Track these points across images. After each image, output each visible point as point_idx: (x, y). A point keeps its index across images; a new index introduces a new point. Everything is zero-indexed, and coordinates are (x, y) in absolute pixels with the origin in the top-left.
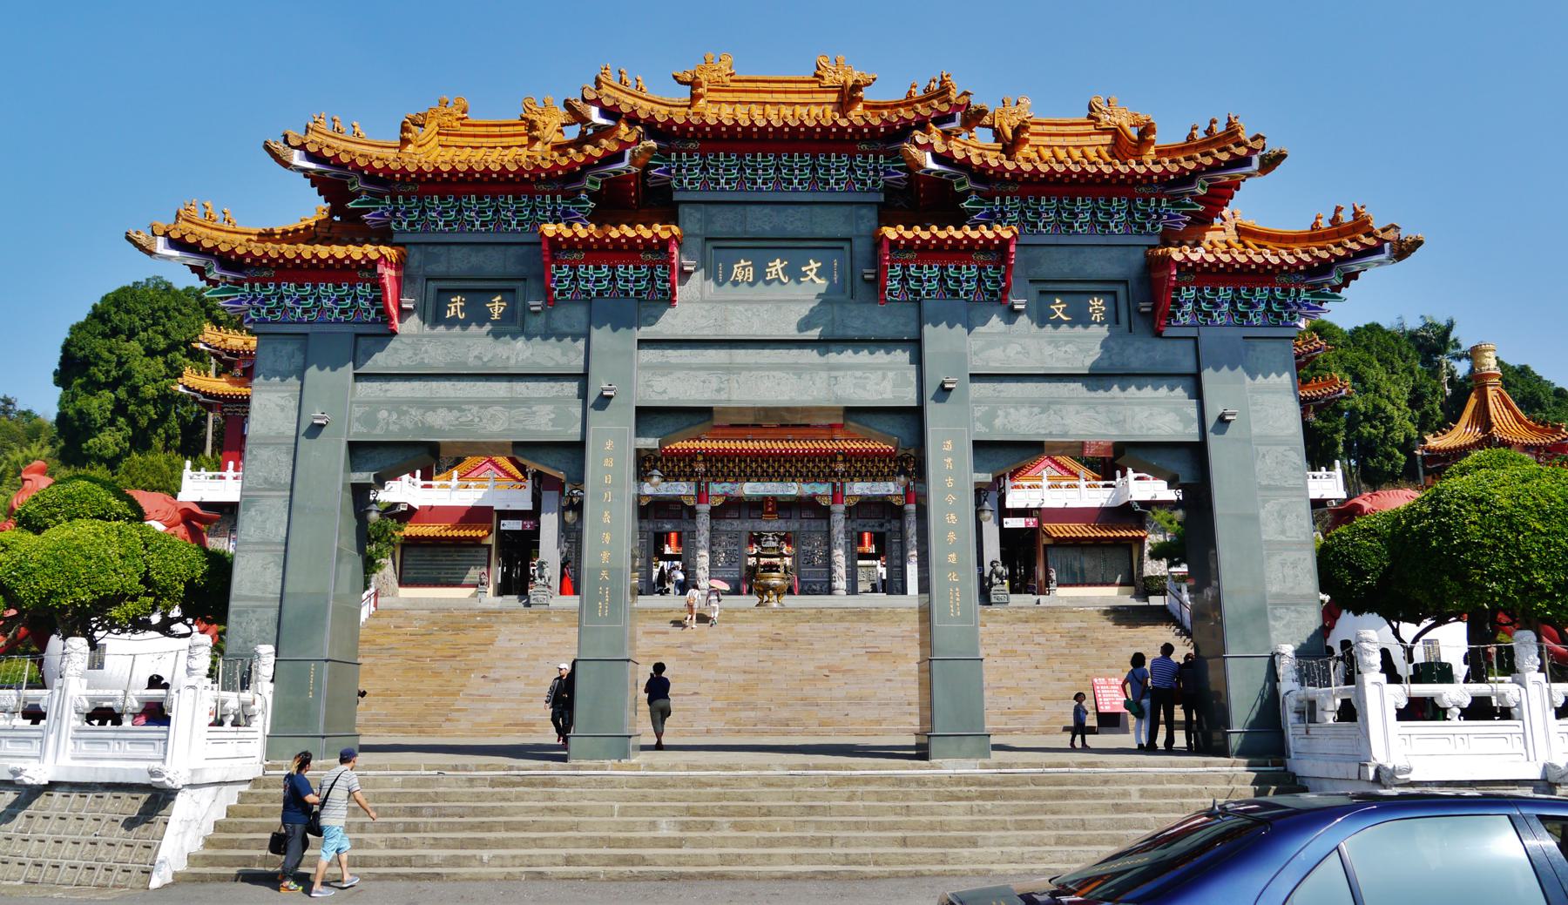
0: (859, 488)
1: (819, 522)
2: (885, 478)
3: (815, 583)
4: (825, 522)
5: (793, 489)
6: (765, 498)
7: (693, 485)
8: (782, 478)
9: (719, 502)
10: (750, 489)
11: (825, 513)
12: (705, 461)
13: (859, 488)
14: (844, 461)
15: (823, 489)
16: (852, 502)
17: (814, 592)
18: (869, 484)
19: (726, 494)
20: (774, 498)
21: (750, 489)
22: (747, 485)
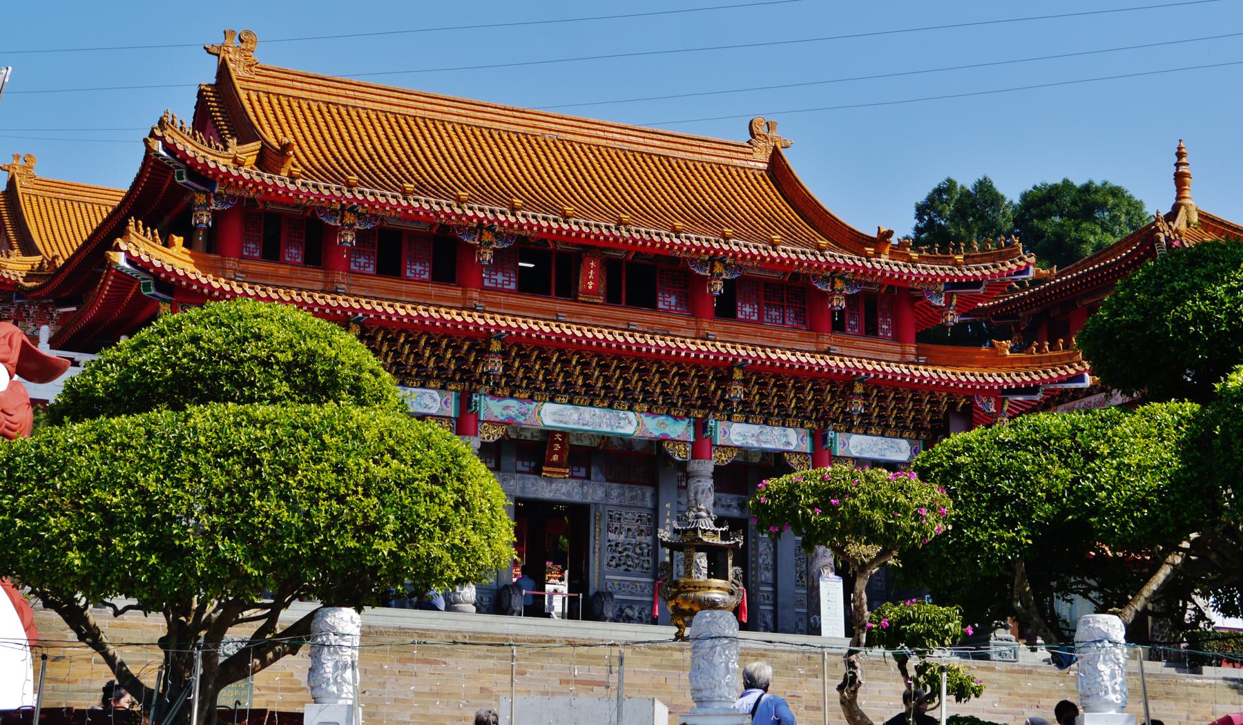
0: (740, 434)
1: (638, 491)
2: (784, 419)
3: (631, 604)
4: (649, 492)
5: (629, 424)
6: (605, 438)
7: (452, 397)
8: (611, 401)
9: (494, 434)
10: (553, 415)
12: (504, 354)
13: (740, 434)
14: (745, 382)
15: (679, 430)
16: (725, 458)
17: (629, 619)
18: (755, 429)
19: (509, 423)
20: (565, 434)
21: (553, 415)
22: (549, 408)
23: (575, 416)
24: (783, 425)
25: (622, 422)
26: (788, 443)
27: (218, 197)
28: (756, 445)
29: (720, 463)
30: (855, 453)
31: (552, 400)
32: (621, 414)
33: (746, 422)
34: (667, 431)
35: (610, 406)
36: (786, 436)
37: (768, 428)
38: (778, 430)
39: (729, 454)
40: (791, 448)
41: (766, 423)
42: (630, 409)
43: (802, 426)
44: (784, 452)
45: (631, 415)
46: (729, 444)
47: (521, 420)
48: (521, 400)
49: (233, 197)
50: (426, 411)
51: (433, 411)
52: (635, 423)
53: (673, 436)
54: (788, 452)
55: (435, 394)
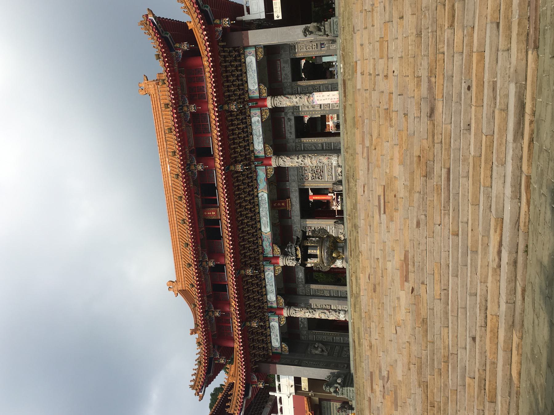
5: (263, 195)
9: (277, 250)
10: (266, 229)
11: (281, 172)
18: (255, 137)
21: (266, 229)
23: (265, 218)
24: (251, 125)
25: (263, 198)
26: (258, 121)
27: (215, 355)
28: (261, 137)
29: (272, 152)
30: (257, 87)
31: (260, 229)
32: (260, 199)
33: (252, 143)
34: (263, 179)
35: (258, 205)
36: (255, 122)
37: (254, 131)
38: (254, 127)
39: (267, 148)
40: (260, 119)
41: (251, 134)
42: (257, 196)
43: (250, 116)
44: (262, 122)
45: (260, 195)
46: (263, 151)
47: (270, 240)
48: (262, 241)
49: (213, 351)
50: (273, 277)
51: (273, 274)
52: (262, 193)
53: (264, 176)
54: (262, 120)
55: (266, 273)
